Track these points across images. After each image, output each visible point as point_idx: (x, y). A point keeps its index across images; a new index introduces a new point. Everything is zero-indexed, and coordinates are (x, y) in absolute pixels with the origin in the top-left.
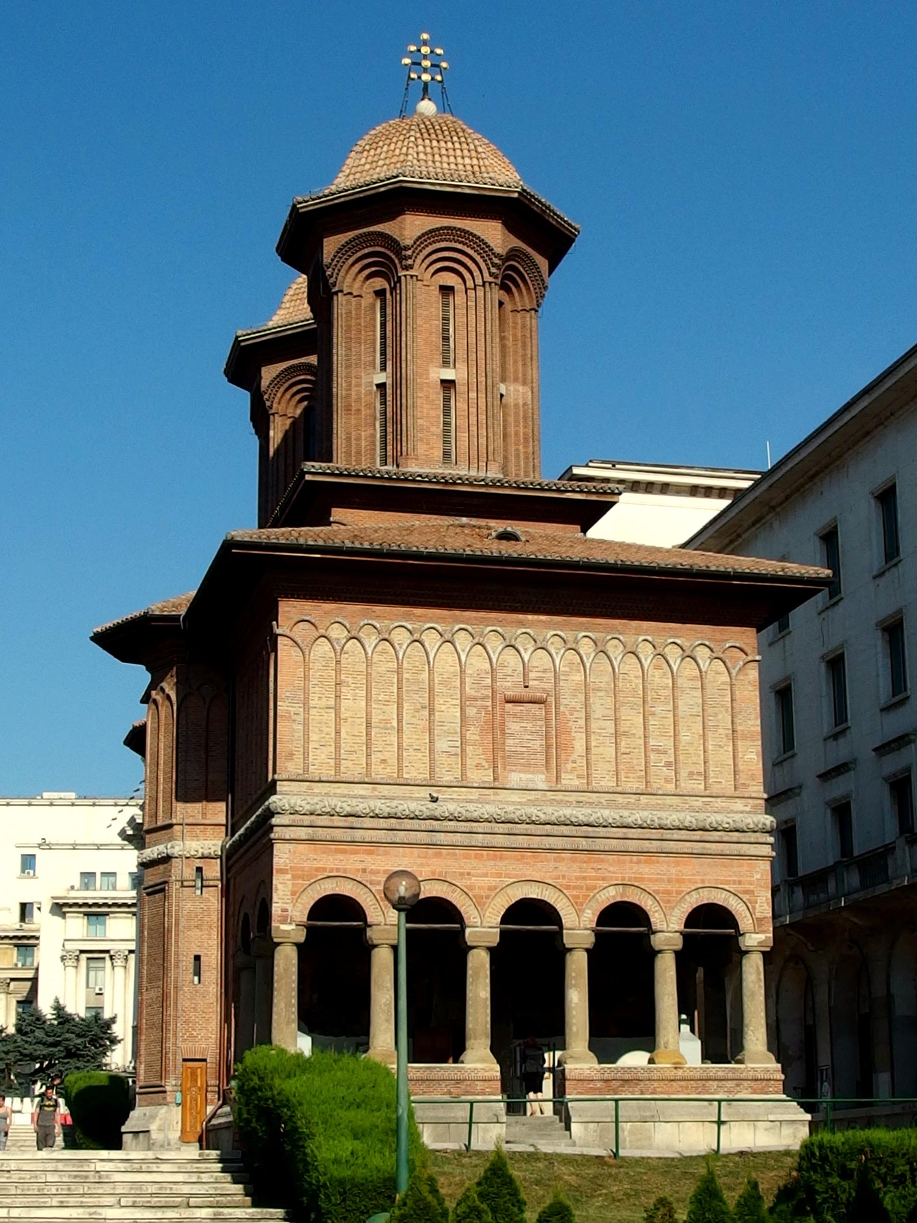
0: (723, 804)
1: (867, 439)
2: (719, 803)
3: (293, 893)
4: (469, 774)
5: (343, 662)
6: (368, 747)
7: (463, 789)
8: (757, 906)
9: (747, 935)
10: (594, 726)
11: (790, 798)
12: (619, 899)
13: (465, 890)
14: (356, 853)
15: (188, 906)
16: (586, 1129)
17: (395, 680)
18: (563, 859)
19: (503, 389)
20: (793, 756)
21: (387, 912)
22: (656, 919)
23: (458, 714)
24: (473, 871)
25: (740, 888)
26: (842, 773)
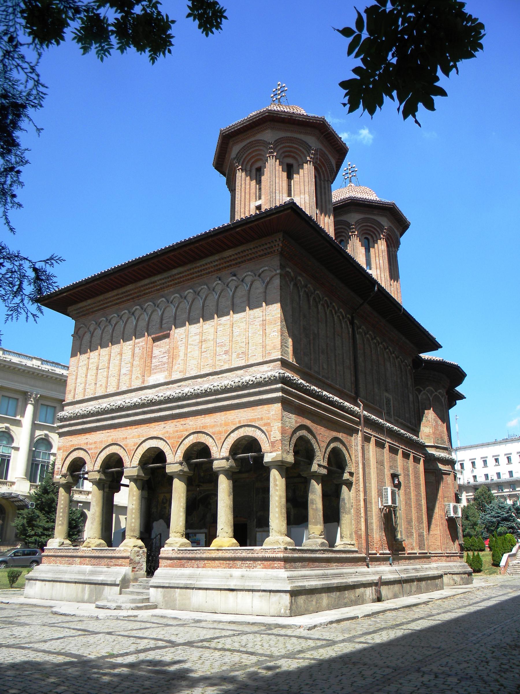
5: (93, 341)
12: (195, 441)
16: (157, 591)
25: (261, 422)
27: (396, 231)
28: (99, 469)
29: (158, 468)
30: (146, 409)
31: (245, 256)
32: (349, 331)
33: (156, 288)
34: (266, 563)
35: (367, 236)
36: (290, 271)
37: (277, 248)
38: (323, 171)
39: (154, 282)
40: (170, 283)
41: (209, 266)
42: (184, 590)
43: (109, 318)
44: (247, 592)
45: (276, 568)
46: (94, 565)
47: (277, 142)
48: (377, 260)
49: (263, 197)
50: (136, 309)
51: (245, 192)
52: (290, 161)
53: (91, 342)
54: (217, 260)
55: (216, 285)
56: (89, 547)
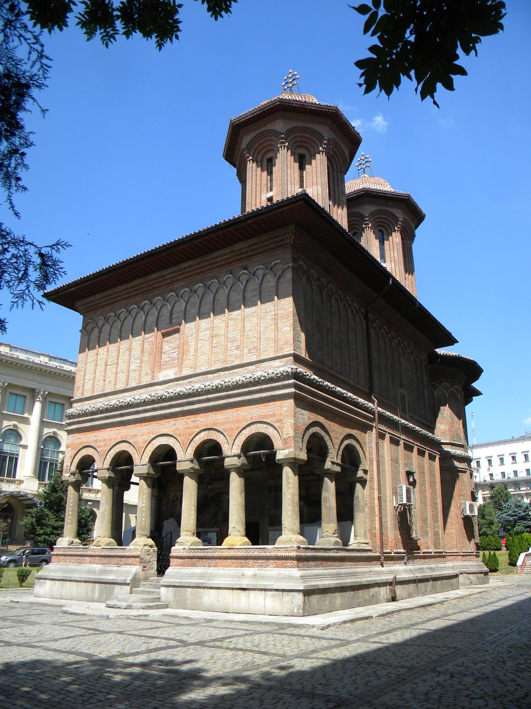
5: (101, 336)
6: (105, 376)
12: (206, 438)
16: (168, 590)
25: (274, 419)
27: (411, 223)
28: (108, 466)
29: (168, 465)
30: (156, 406)
31: (256, 249)
32: (363, 326)
33: (165, 282)
34: (278, 562)
35: (381, 228)
36: (302, 263)
37: (289, 241)
38: (336, 162)
39: (163, 276)
40: (180, 277)
41: (219, 259)
42: (195, 589)
43: (117, 314)
44: (259, 592)
45: (289, 567)
46: (104, 564)
47: (289, 133)
48: (392, 253)
49: (274, 188)
50: (145, 304)
51: (256, 184)
52: (302, 151)
53: (99, 337)
54: (228, 254)
55: (227, 278)
56: (99, 546)
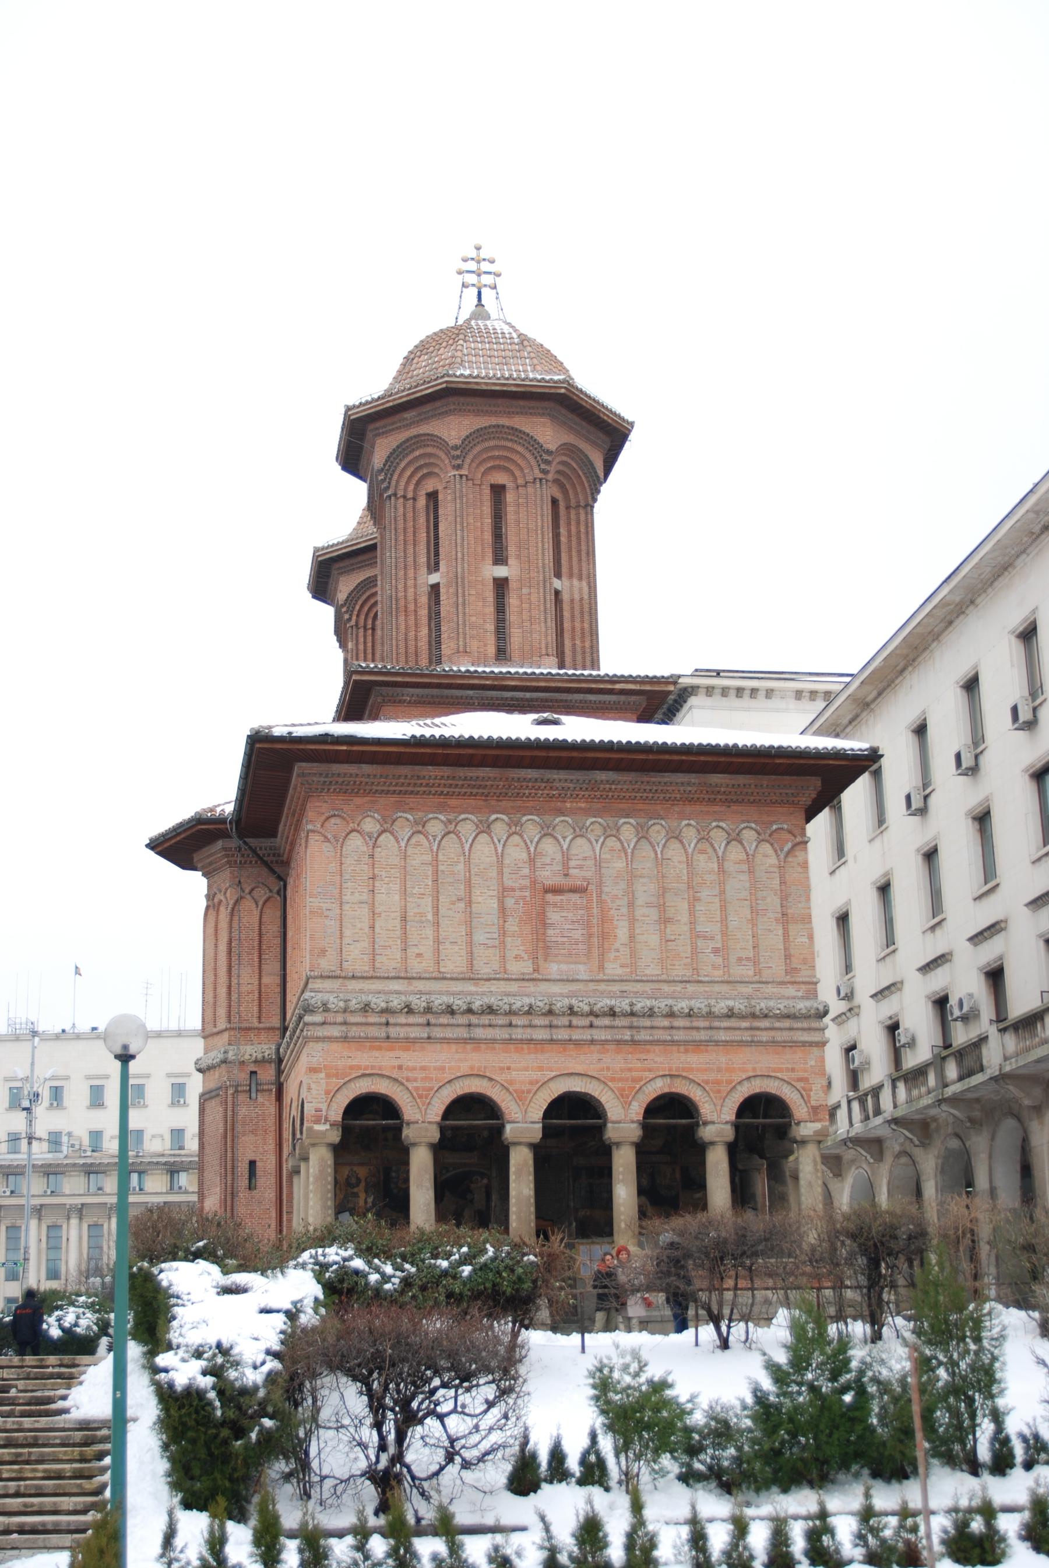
0: (775, 990)
1: (951, 629)
2: (770, 989)
3: (327, 1093)
4: (509, 967)
5: (376, 855)
7: (502, 982)
8: (812, 1093)
9: (802, 1124)
10: (639, 912)
11: (892, 993)
12: (666, 1090)
13: (505, 1084)
14: (392, 1049)
15: (243, 1111)
17: (430, 873)
18: (608, 1051)
19: (557, 584)
20: (894, 951)
21: (426, 1110)
22: (706, 1109)
23: (495, 906)
24: (513, 1066)
25: (794, 1075)
26: (939, 966)
28: (438, 1119)
